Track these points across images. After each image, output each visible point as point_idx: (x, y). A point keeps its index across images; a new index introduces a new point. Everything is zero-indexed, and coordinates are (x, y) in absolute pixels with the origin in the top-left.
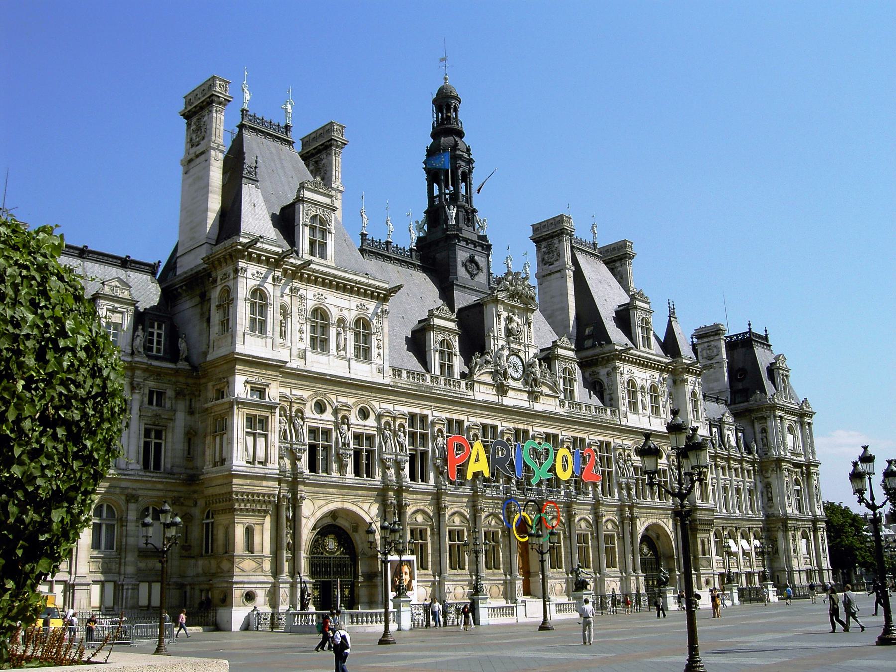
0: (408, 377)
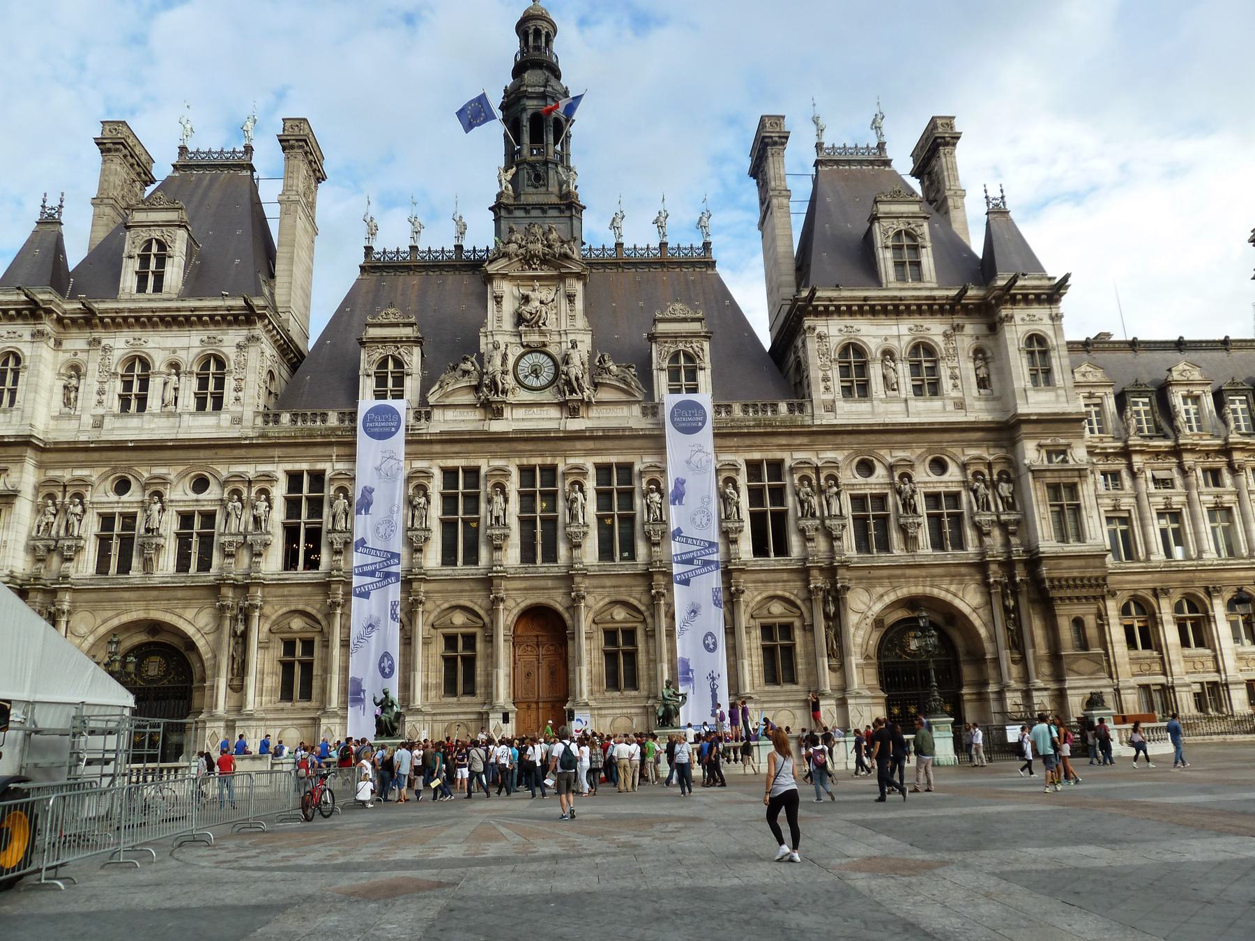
0: (294, 421)
